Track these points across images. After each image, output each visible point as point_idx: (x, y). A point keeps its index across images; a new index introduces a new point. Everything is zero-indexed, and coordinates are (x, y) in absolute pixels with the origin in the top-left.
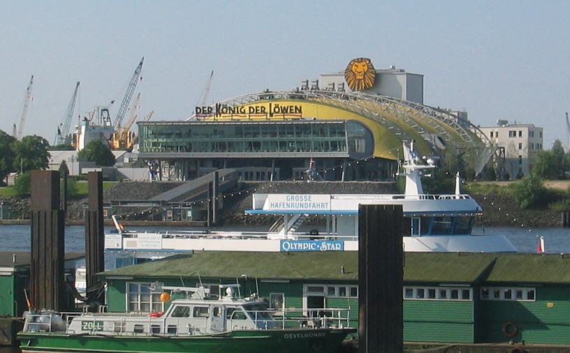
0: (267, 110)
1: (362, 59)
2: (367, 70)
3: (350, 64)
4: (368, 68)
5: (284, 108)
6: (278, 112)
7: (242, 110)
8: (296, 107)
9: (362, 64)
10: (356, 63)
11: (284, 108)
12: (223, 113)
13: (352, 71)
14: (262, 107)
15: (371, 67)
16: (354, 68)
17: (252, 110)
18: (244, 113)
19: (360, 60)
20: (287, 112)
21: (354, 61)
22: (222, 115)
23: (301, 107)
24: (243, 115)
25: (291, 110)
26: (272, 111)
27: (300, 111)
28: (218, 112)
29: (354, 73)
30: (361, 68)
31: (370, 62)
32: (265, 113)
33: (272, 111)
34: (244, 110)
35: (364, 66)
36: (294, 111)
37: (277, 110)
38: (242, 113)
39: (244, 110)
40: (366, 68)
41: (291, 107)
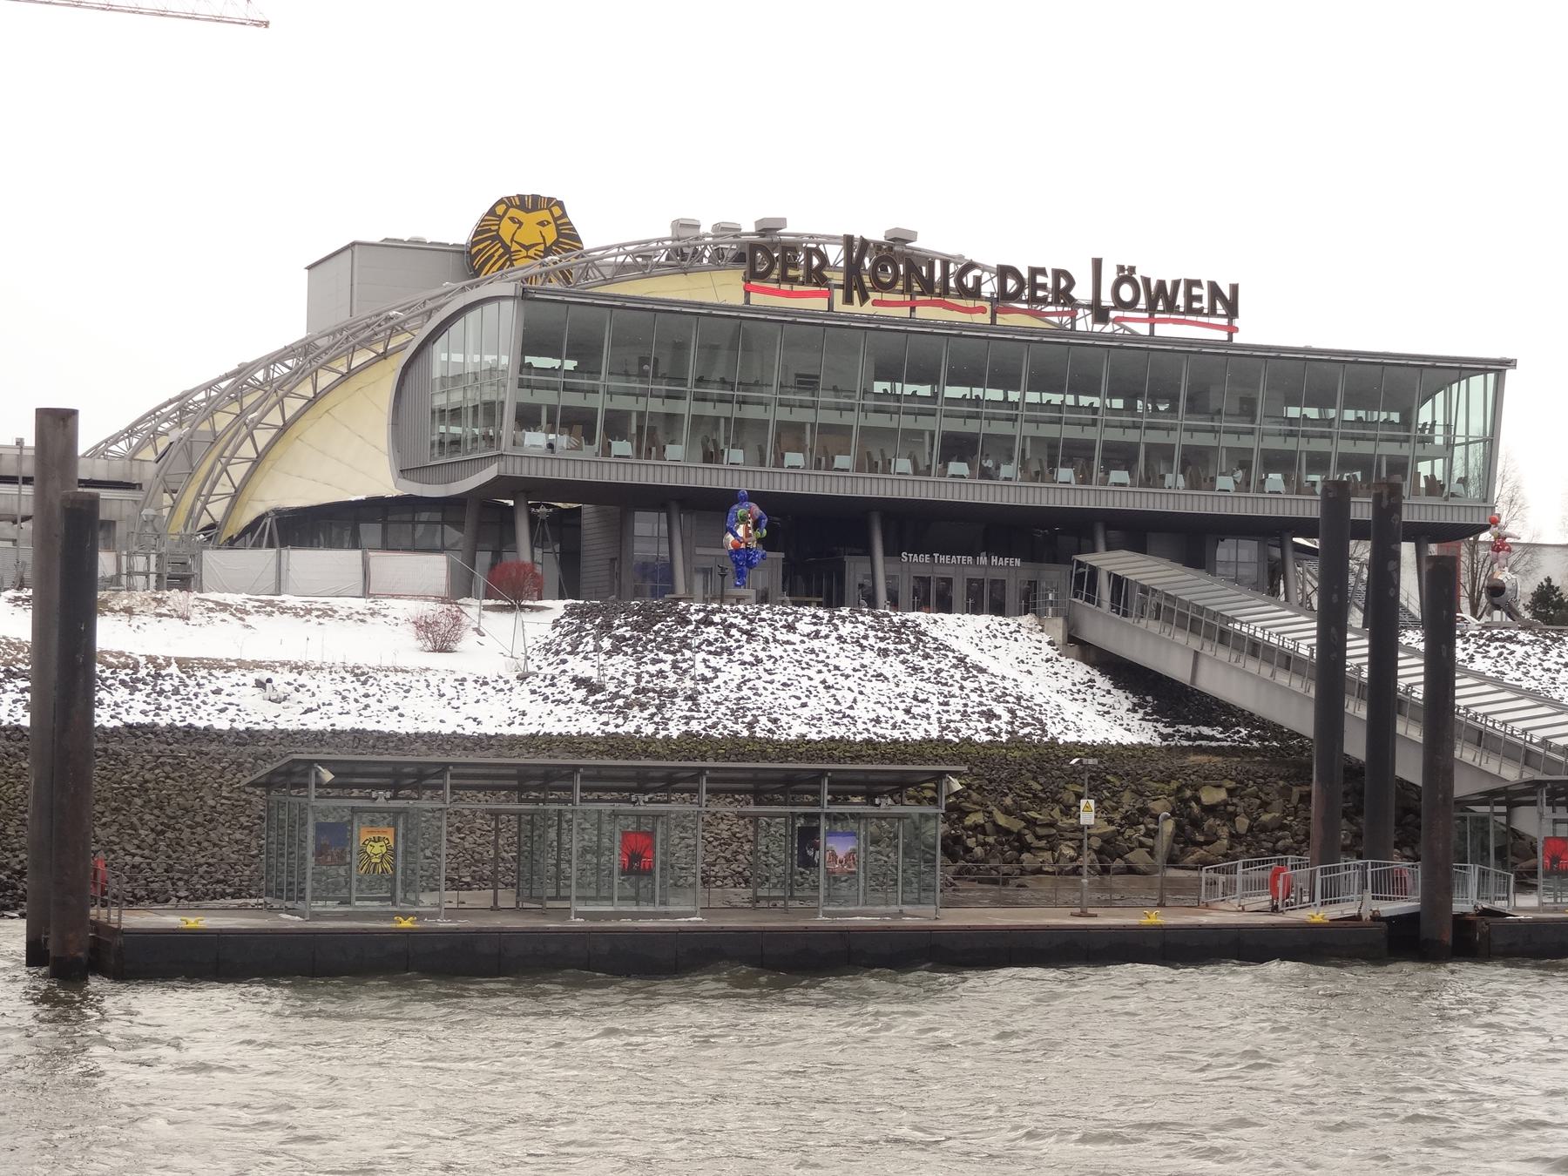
0: (1082, 292)
1: (536, 198)
2: (556, 243)
3: (492, 212)
4: (560, 235)
5: (1161, 284)
6: (1131, 306)
7: (969, 281)
8: (1214, 290)
9: (544, 215)
10: (513, 212)
11: (1161, 284)
12: (881, 287)
13: (497, 238)
14: (1058, 274)
15: (567, 237)
16: (506, 230)
17: (1011, 285)
18: (975, 293)
19: (531, 204)
20: (1171, 307)
21: (507, 202)
22: (874, 296)
23: (1235, 289)
24: (970, 303)
25: (1190, 298)
26: (1107, 299)
27: (1232, 309)
28: (854, 284)
29: (507, 248)
30: (531, 230)
31: (564, 215)
32: (1071, 301)
33: (1107, 299)
34: (978, 280)
35: (542, 224)
36: (1205, 304)
37: (1126, 293)
38: (964, 292)
39: (978, 280)
40: (551, 234)
41: (1191, 283)
